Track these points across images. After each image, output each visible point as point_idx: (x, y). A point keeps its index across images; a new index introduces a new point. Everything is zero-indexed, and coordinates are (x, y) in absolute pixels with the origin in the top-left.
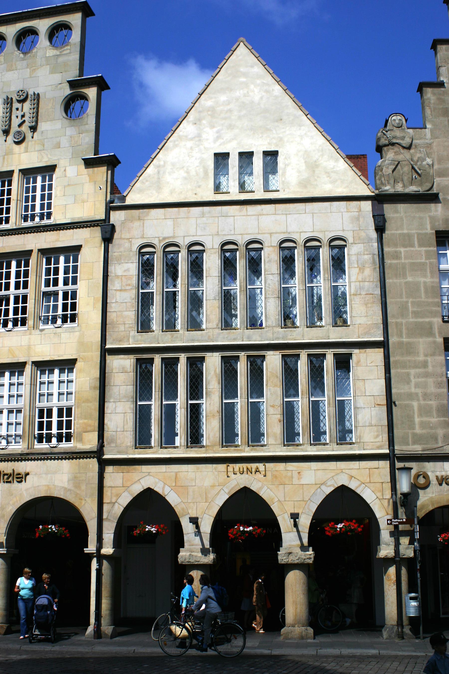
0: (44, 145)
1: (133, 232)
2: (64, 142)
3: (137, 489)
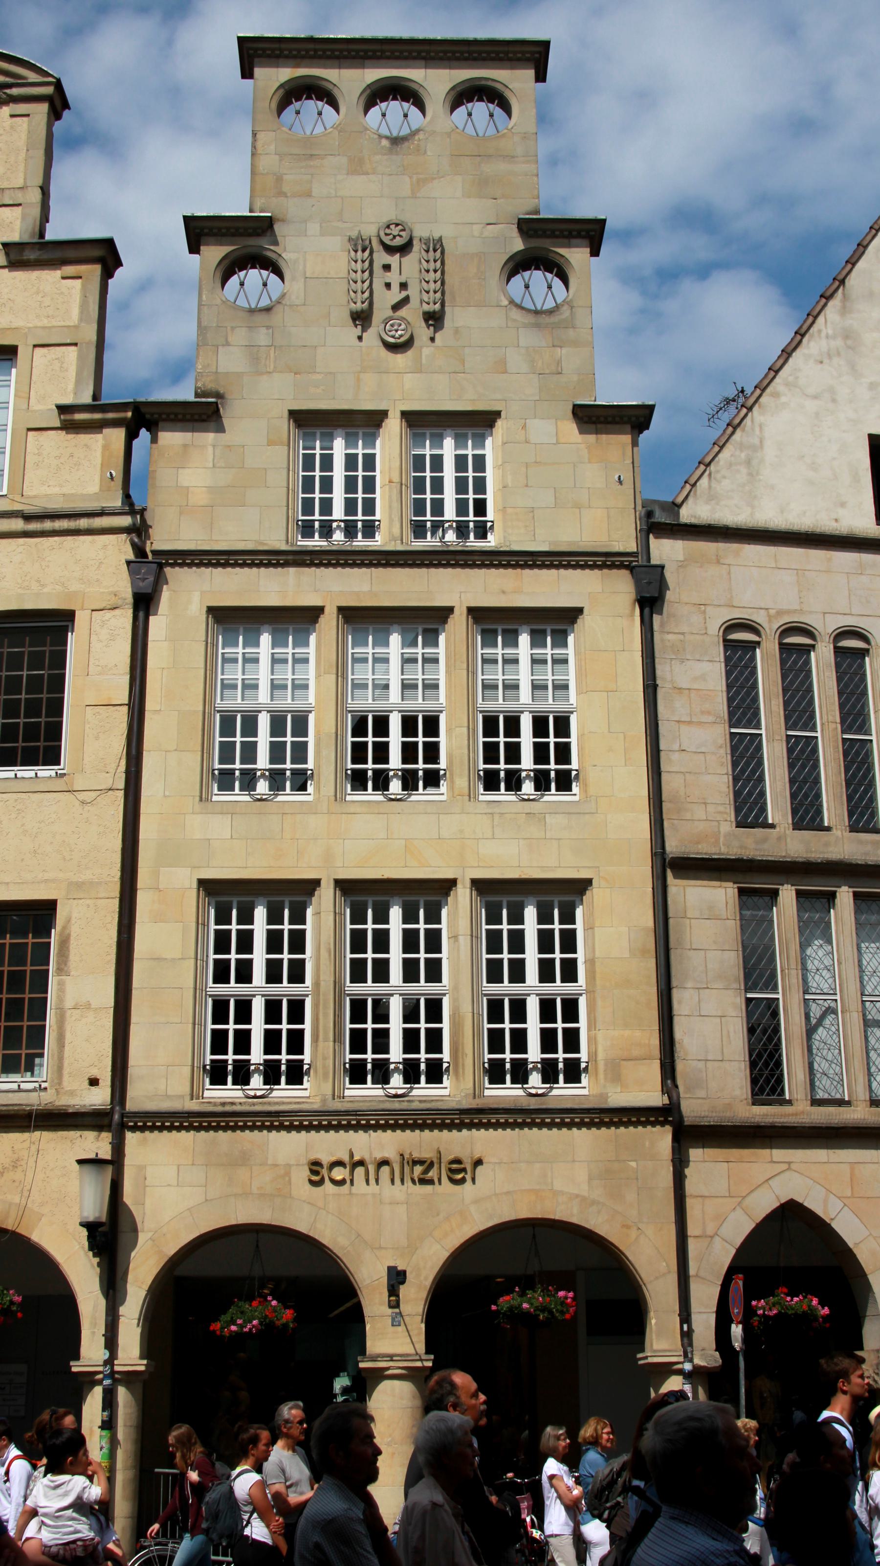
0: (463, 362)
1: (712, 588)
2: (516, 361)
3: (765, 1203)
